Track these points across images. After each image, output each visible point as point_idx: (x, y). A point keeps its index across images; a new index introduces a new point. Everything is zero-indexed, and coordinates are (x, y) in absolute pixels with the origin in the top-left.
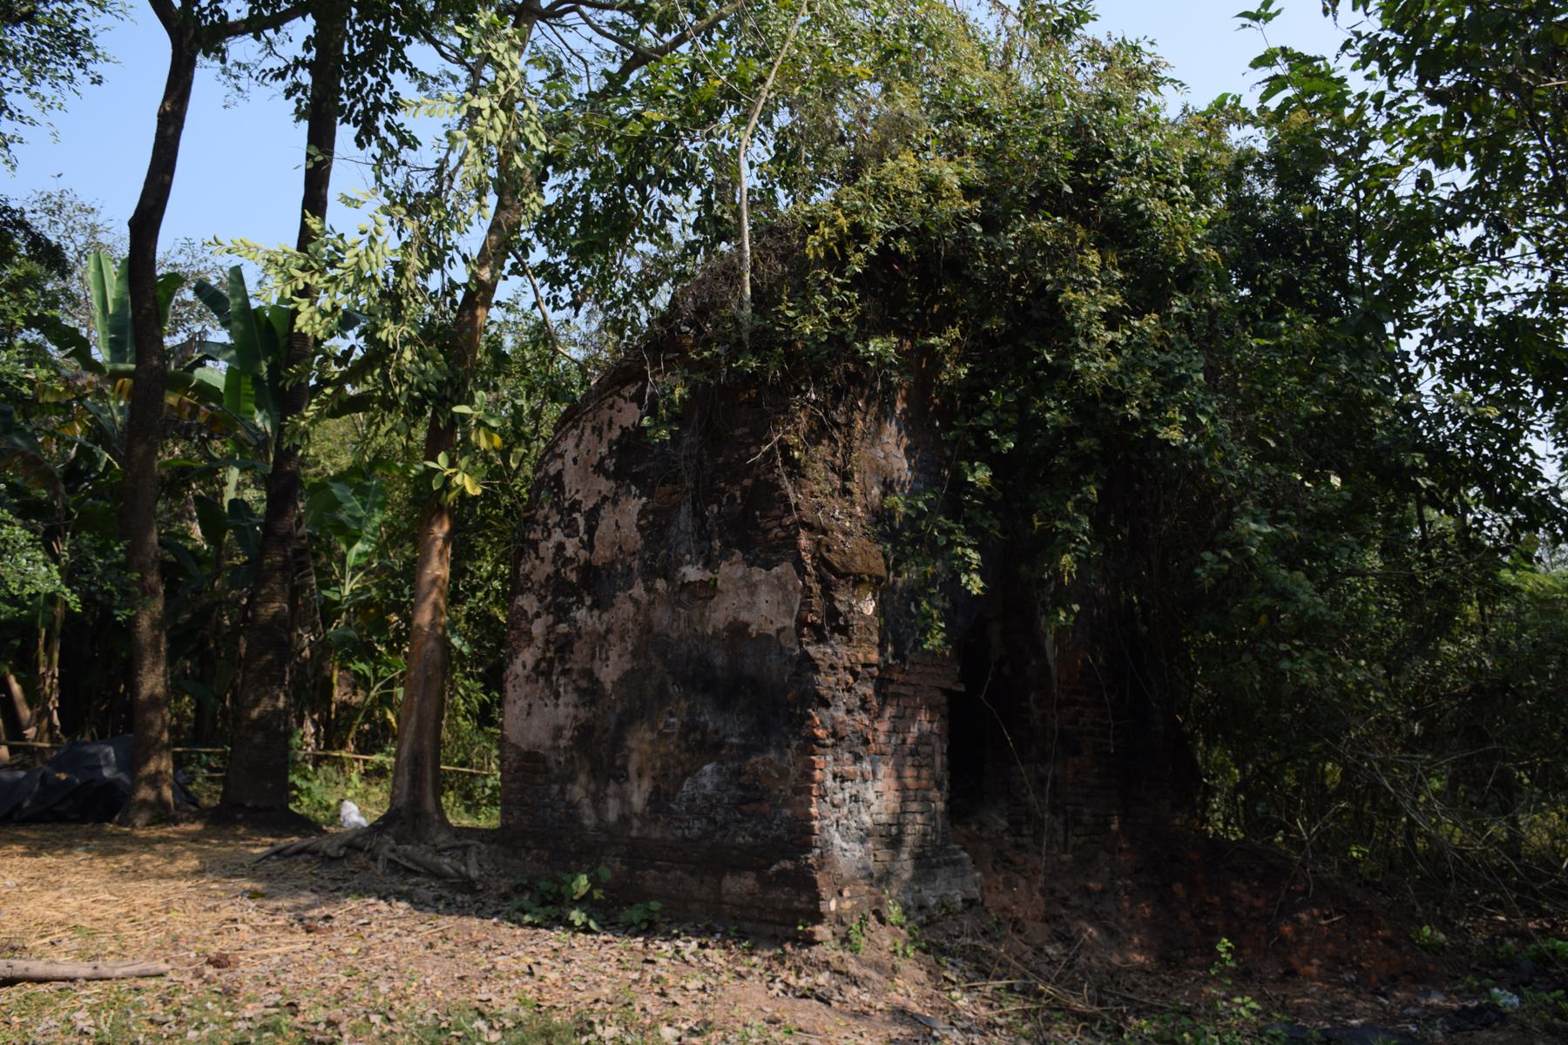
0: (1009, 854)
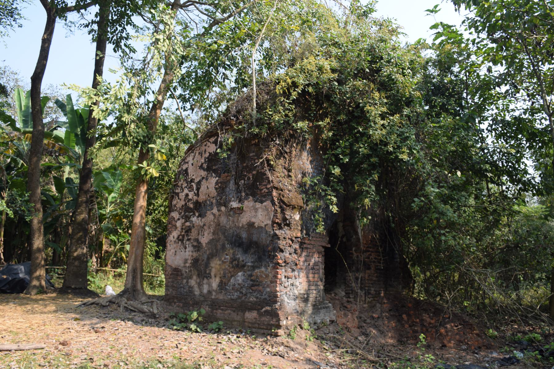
0: (345, 305)
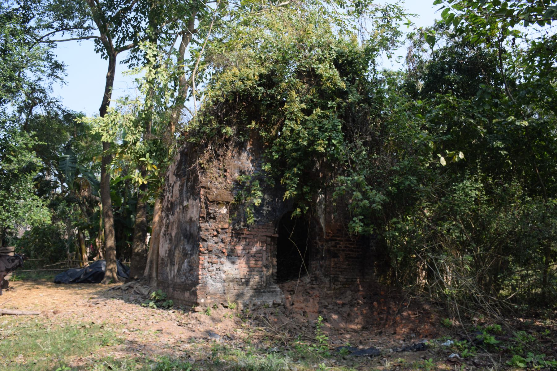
0: (309, 291)
